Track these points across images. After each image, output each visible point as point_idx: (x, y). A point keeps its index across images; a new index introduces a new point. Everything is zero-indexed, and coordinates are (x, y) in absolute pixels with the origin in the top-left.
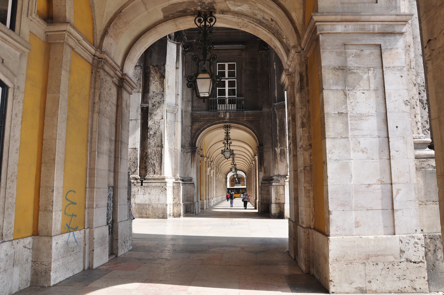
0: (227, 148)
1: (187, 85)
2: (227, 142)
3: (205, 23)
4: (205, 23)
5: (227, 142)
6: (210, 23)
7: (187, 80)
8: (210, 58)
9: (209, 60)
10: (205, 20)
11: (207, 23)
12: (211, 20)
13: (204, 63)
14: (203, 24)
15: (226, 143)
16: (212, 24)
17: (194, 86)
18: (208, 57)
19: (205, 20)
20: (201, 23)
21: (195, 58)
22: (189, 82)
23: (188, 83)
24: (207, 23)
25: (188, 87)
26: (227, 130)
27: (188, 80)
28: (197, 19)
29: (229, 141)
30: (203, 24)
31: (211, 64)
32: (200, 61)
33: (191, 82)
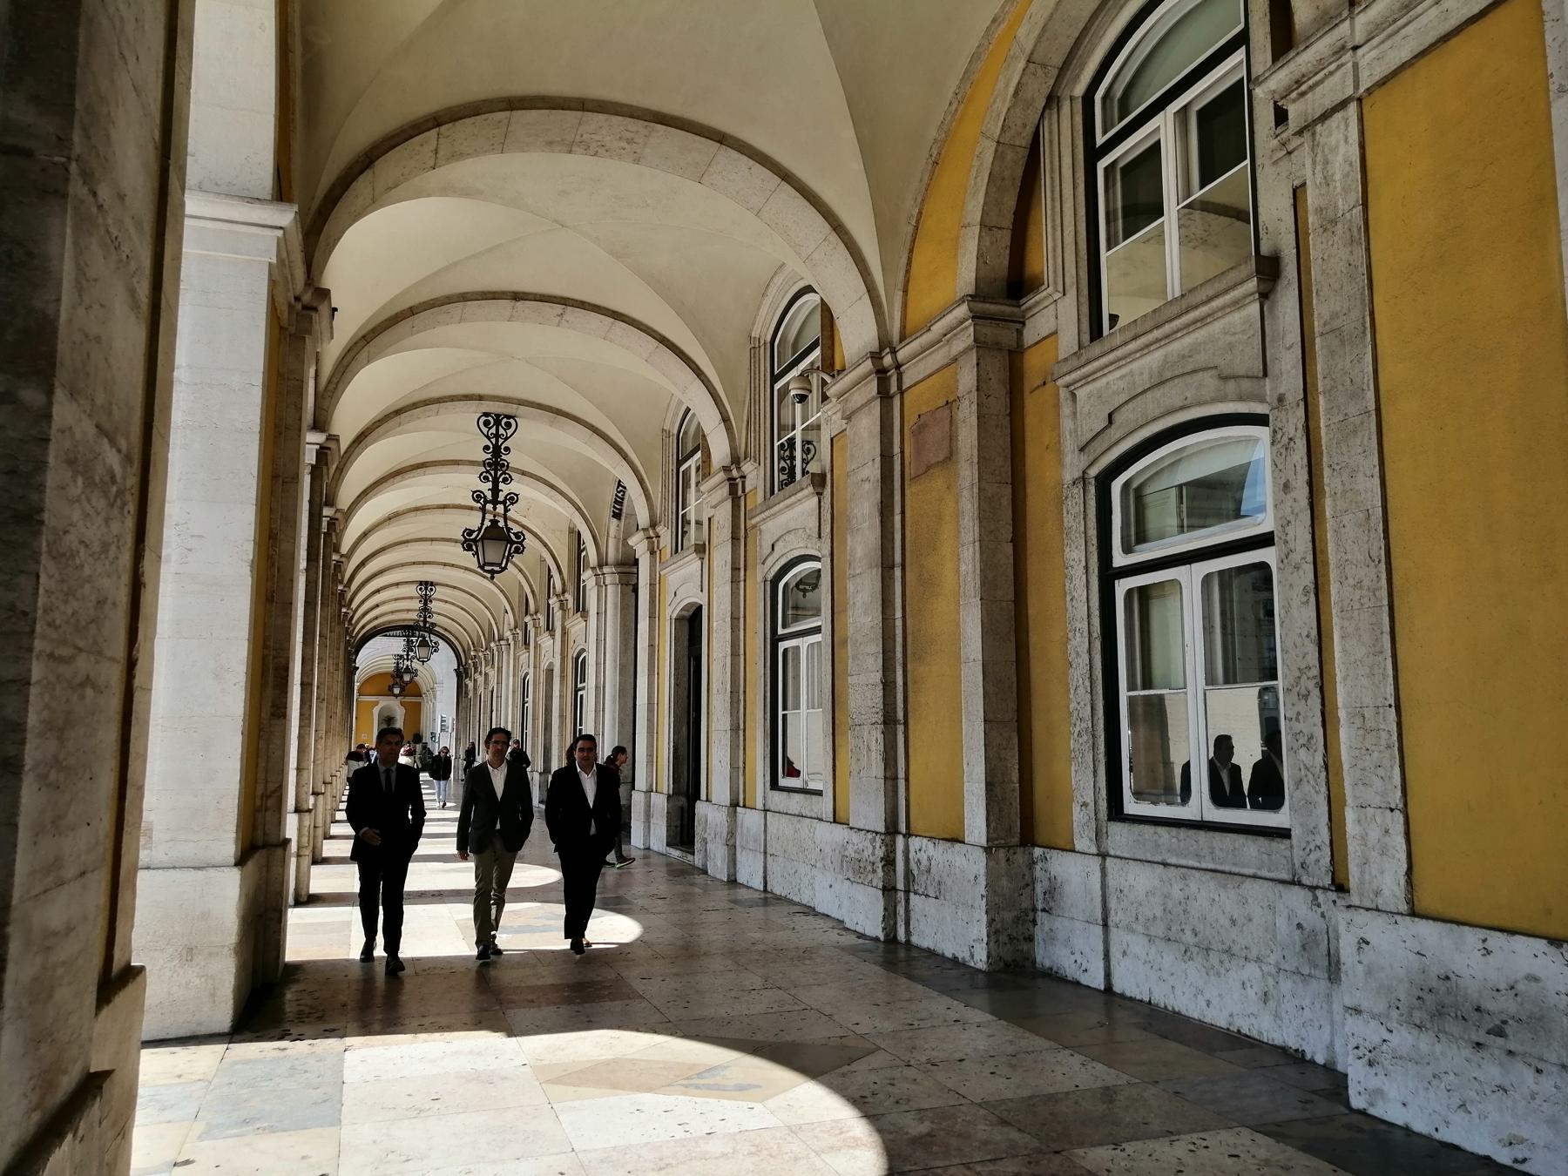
9: (504, 503)
11: (501, 431)
12: (509, 425)
16: (510, 432)
18: (501, 498)
30: (493, 430)
31: (506, 510)
32: (486, 501)
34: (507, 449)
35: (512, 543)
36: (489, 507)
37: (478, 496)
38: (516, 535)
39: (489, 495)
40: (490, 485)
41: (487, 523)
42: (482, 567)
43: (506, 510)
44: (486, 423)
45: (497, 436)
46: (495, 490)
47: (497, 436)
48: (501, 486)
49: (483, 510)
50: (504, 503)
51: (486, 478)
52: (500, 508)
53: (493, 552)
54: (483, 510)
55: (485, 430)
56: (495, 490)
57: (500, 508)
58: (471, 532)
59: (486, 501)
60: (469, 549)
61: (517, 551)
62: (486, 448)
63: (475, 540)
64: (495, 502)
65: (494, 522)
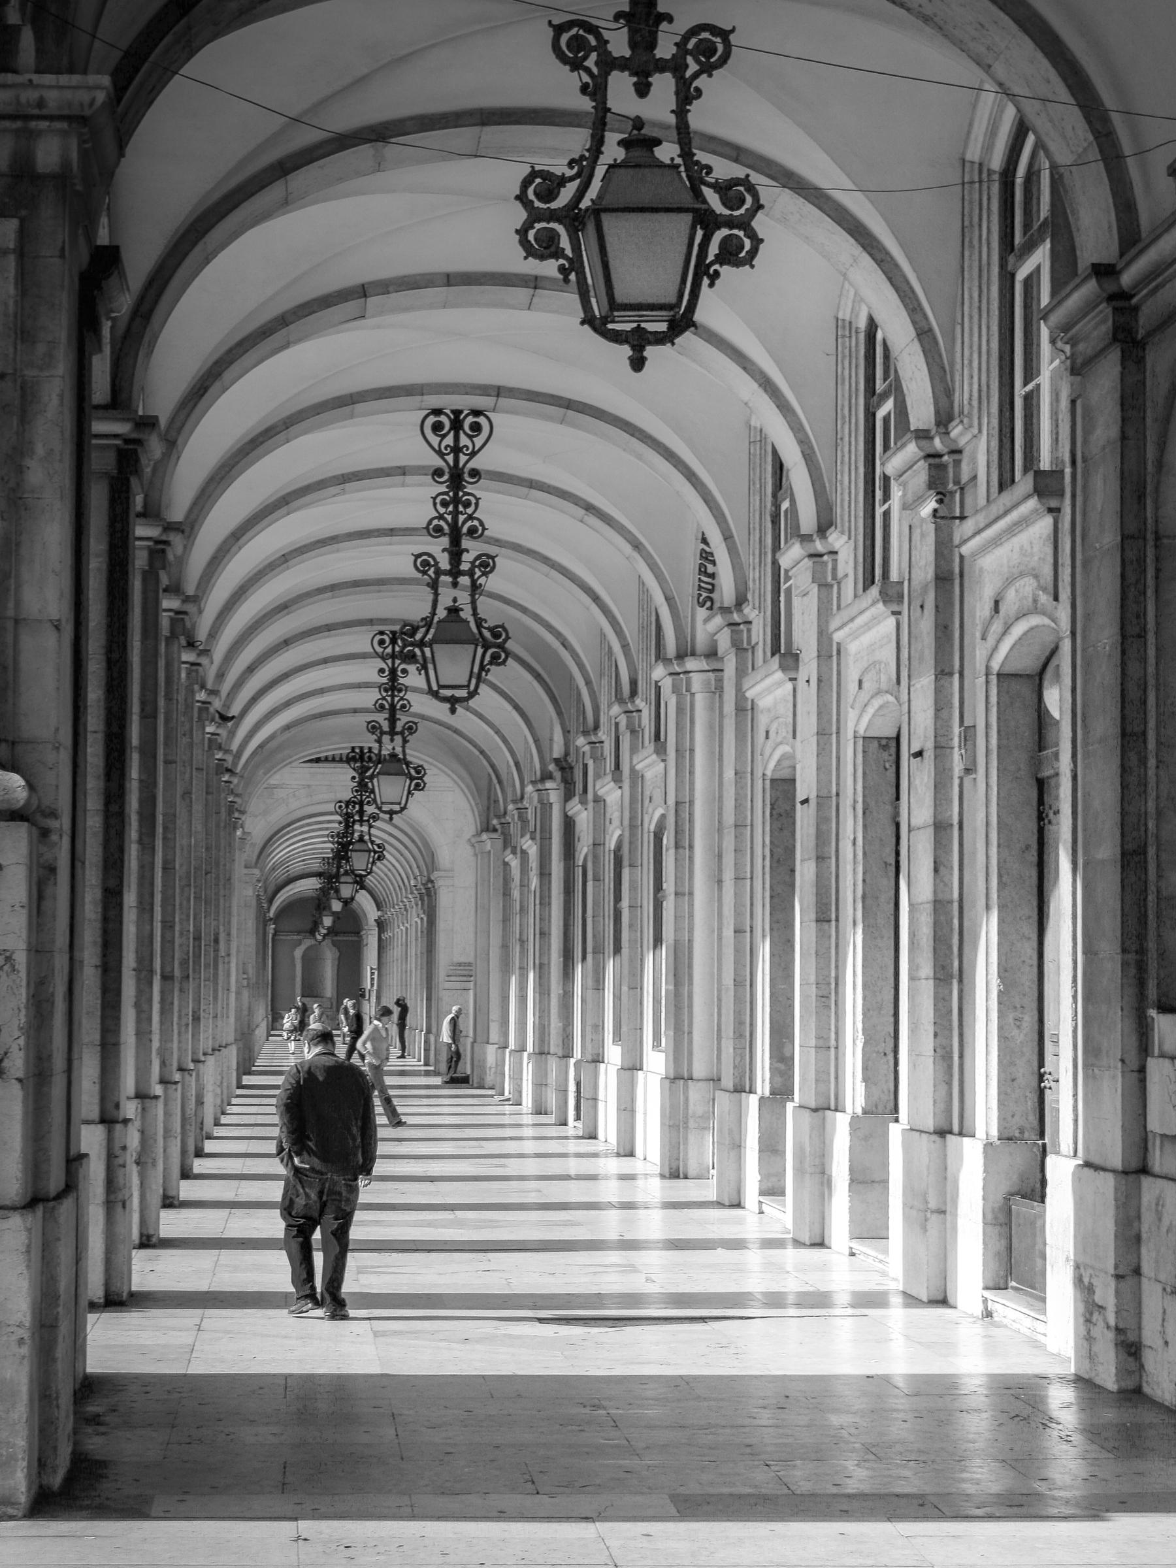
0: (454, 611)
1: (522, 233)
2: (456, 553)
5: (456, 553)
7: (522, 198)
8: (681, 45)
9: (676, 67)
13: (642, 90)
15: (445, 564)
17: (565, 243)
18: (665, 49)
21: (577, 44)
22: (535, 215)
25: (530, 252)
26: (456, 450)
29: (472, 549)
32: (609, 64)
33: (552, 216)
36: (620, 85)
38: (725, 189)
39: (619, 44)
41: (613, 151)
42: (597, 324)
43: (686, 95)
49: (596, 90)
52: (664, 85)
54: (596, 90)
57: (664, 85)
58: (550, 185)
59: (609, 64)
60: (547, 248)
61: (731, 255)
65: (640, 141)
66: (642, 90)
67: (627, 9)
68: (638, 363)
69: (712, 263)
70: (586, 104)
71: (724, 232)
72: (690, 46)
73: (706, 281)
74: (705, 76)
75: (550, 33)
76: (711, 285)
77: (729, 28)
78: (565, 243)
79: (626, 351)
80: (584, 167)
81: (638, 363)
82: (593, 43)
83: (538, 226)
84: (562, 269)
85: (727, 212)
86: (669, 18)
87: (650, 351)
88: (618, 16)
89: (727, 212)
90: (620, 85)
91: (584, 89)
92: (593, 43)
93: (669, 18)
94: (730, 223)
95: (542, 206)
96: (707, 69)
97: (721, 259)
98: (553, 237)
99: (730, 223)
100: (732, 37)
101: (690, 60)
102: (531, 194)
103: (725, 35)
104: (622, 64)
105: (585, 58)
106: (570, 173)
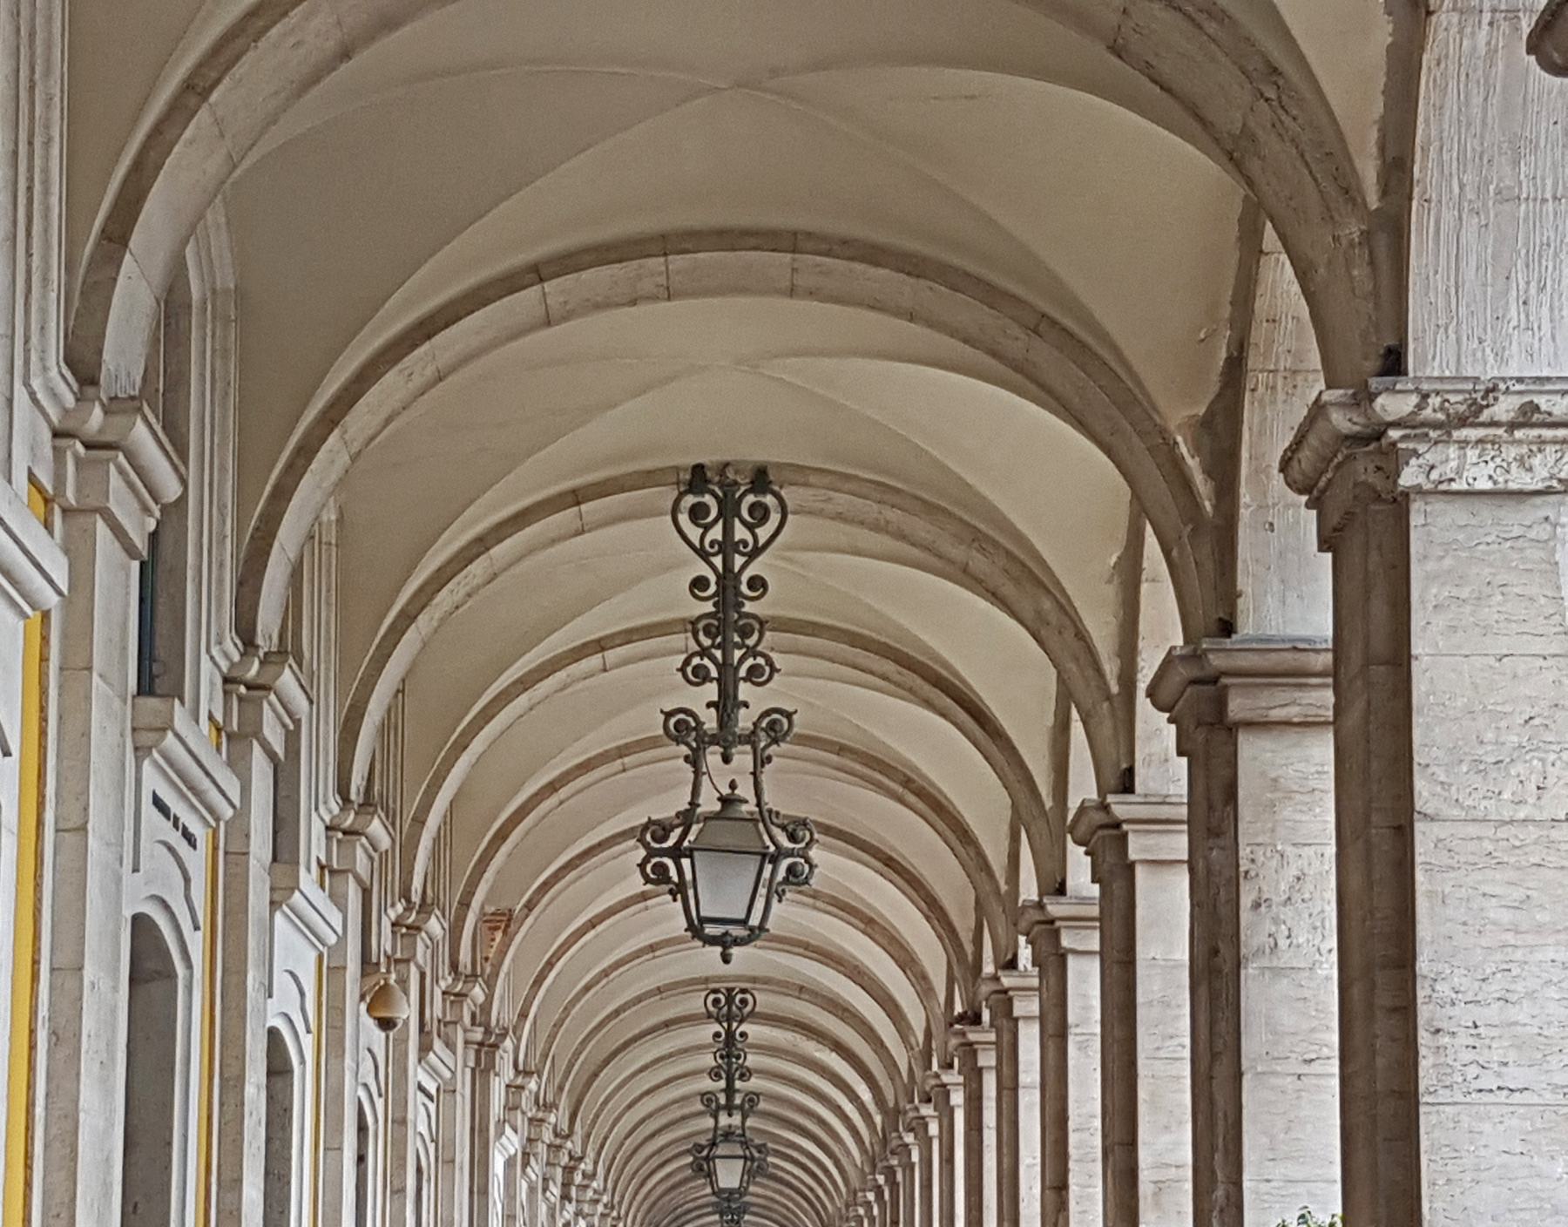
1: (642, 866)
3: (728, 531)
4: (728, 531)
6: (751, 528)
9: (750, 739)
10: (728, 511)
11: (740, 533)
12: (760, 514)
13: (726, 759)
14: (716, 533)
16: (764, 533)
17: (673, 873)
19: (728, 511)
20: (707, 528)
22: (651, 853)
23: (646, 861)
24: (740, 533)
25: (648, 880)
27: (646, 846)
28: (690, 500)
30: (716, 533)
31: (761, 761)
32: (705, 740)
34: (757, 583)
35: (781, 853)
37: (681, 727)
39: (710, 720)
40: (711, 691)
41: (709, 803)
43: (761, 761)
44: (697, 513)
45: (727, 546)
46: (726, 705)
47: (727, 546)
48: (745, 691)
49: (694, 760)
50: (750, 739)
51: (701, 676)
53: (724, 891)
55: (694, 533)
56: (726, 705)
59: (705, 740)
62: (699, 583)
63: (677, 853)
64: (726, 739)
66: (726, 759)
67: (716, 698)
68: (726, 959)
69: (780, 884)
70: (689, 768)
71: (789, 861)
72: (764, 725)
73: (776, 898)
74: (774, 747)
75: (662, 717)
76: (780, 901)
77: (791, 709)
78: (673, 873)
79: (719, 949)
80: (687, 818)
81: (726, 959)
82: (693, 724)
83: (654, 861)
84: (670, 892)
85: (791, 846)
86: (746, 705)
87: (735, 951)
88: (709, 705)
89: (791, 846)
90: (713, 757)
91: (686, 759)
92: (693, 724)
93: (746, 705)
94: (790, 853)
95: (657, 846)
96: (775, 741)
97: (786, 881)
98: (665, 868)
99: (790, 853)
100: (795, 717)
101: (762, 734)
102: (648, 837)
103: (789, 715)
104: (714, 740)
105: (688, 735)
106: (677, 822)
